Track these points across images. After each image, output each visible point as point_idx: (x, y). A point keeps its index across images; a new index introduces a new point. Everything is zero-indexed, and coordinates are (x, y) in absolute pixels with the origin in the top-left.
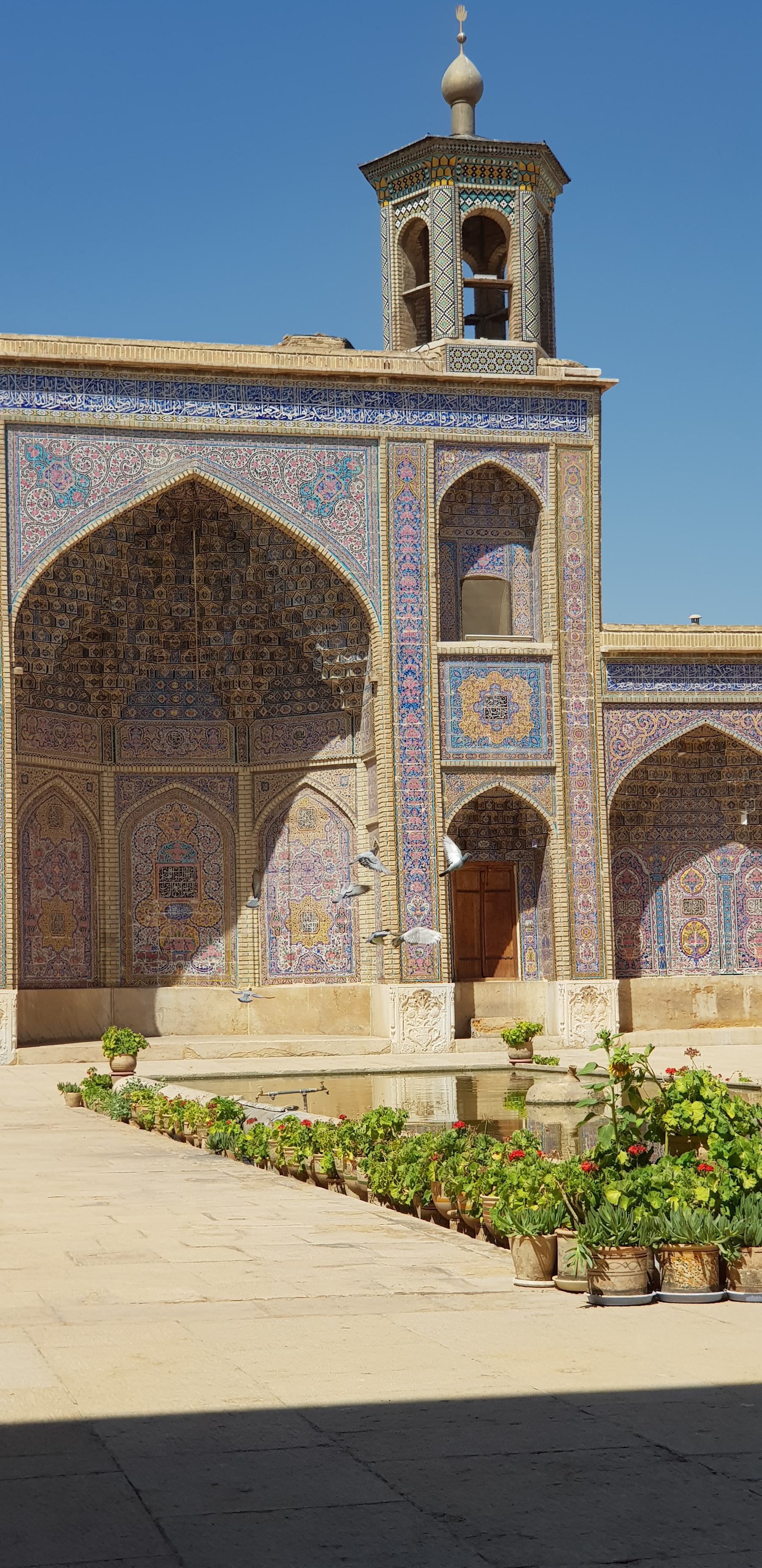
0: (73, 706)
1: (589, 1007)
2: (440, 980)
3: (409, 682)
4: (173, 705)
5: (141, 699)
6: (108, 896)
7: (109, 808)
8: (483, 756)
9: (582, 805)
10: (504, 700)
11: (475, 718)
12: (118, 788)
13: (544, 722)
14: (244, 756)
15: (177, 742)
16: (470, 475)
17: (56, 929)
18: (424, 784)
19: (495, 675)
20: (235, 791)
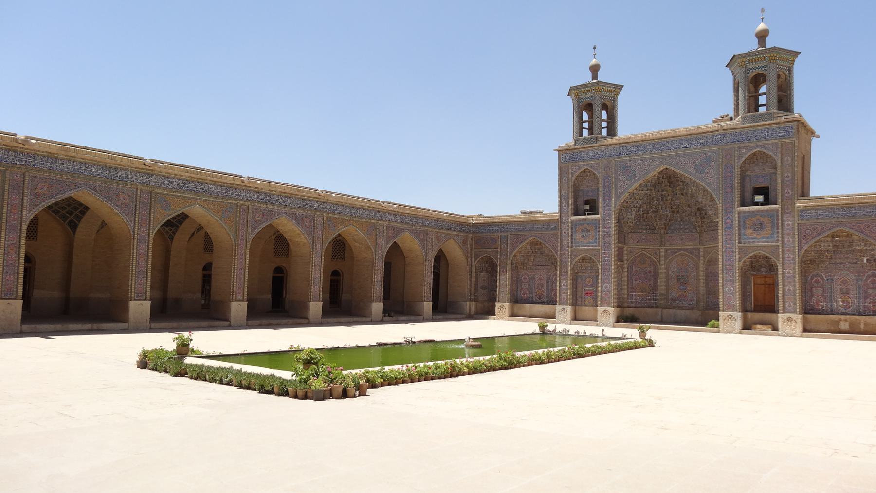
10: (761, 225)
14: (701, 243)
17: (642, 292)
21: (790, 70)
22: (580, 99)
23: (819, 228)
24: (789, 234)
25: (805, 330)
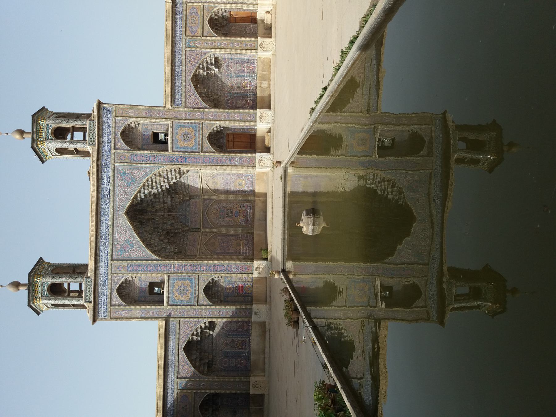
0: (186, 239)
1: (264, 118)
2: (256, 157)
3: (179, 160)
4: (186, 214)
5: (184, 222)
6: (232, 231)
7: (211, 230)
8: (199, 141)
9: (212, 116)
11: (189, 143)
12: (206, 228)
13: (190, 124)
15: (195, 213)
16: (124, 140)
18: (206, 158)
19: (177, 137)
20: (208, 199)
21: (56, 114)
22: (43, 297)
23: (190, 94)
24: (193, 115)
25: (269, 108)
